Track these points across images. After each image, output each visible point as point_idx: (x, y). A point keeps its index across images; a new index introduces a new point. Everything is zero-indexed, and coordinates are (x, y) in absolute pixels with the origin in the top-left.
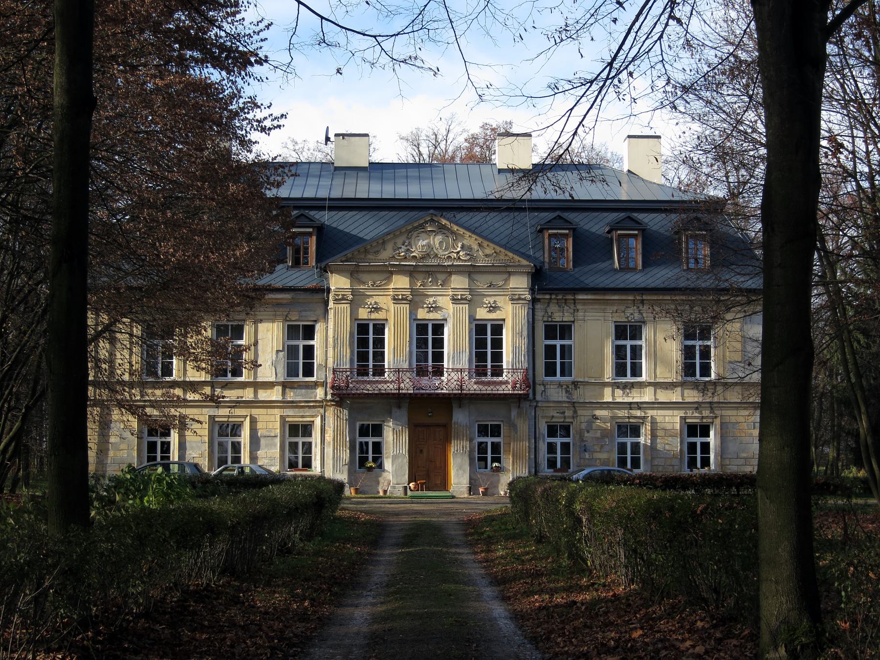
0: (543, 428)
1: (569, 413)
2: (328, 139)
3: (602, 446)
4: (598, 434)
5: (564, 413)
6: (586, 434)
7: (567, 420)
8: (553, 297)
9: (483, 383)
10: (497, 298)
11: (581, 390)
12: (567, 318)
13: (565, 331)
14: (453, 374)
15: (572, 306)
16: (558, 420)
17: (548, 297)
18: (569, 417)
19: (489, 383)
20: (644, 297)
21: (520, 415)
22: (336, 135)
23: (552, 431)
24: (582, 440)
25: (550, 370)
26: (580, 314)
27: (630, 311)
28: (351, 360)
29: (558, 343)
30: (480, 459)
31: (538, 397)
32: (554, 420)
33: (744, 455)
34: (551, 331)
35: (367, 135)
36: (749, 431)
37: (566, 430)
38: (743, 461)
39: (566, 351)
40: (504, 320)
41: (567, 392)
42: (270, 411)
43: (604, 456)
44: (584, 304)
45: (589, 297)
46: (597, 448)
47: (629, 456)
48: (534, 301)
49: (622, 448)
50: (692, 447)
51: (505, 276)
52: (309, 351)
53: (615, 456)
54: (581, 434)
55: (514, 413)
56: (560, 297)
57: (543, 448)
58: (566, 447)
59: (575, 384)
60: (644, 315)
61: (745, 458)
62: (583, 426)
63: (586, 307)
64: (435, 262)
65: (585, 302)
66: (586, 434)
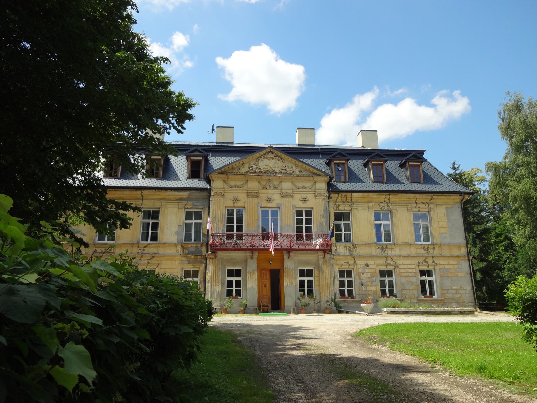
1: (351, 263)
2: (213, 130)
3: (372, 283)
4: (369, 275)
5: (348, 263)
6: (362, 275)
7: (351, 267)
13: (346, 216)
14: (285, 238)
16: (345, 267)
19: (305, 244)
22: (217, 127)
24: (360, 279)
25: (339, 239)
28: (223, 231)
29: (343, 222)
30: (301, 290)
31: (333, 252)
33: (455, 288)
34: (338, 216)
35: (233, 127)
36: (456, 274)
37: (349, 273)
38: (454, 292)
39: (348, 227)
40: (312, 208)
41: (349, 250)
42: (173, 262)
43: (373, 288)
47: (387, 288)
48: (329, 197)
49: (382, 283)
50: (423, 283)
53: (379, 288)
54: (359, 275)
57: (337, 284)
58: (350, 283)
59: (354, 246)
61: (456, 290)
62: (360, 270)
66: (362, 275)
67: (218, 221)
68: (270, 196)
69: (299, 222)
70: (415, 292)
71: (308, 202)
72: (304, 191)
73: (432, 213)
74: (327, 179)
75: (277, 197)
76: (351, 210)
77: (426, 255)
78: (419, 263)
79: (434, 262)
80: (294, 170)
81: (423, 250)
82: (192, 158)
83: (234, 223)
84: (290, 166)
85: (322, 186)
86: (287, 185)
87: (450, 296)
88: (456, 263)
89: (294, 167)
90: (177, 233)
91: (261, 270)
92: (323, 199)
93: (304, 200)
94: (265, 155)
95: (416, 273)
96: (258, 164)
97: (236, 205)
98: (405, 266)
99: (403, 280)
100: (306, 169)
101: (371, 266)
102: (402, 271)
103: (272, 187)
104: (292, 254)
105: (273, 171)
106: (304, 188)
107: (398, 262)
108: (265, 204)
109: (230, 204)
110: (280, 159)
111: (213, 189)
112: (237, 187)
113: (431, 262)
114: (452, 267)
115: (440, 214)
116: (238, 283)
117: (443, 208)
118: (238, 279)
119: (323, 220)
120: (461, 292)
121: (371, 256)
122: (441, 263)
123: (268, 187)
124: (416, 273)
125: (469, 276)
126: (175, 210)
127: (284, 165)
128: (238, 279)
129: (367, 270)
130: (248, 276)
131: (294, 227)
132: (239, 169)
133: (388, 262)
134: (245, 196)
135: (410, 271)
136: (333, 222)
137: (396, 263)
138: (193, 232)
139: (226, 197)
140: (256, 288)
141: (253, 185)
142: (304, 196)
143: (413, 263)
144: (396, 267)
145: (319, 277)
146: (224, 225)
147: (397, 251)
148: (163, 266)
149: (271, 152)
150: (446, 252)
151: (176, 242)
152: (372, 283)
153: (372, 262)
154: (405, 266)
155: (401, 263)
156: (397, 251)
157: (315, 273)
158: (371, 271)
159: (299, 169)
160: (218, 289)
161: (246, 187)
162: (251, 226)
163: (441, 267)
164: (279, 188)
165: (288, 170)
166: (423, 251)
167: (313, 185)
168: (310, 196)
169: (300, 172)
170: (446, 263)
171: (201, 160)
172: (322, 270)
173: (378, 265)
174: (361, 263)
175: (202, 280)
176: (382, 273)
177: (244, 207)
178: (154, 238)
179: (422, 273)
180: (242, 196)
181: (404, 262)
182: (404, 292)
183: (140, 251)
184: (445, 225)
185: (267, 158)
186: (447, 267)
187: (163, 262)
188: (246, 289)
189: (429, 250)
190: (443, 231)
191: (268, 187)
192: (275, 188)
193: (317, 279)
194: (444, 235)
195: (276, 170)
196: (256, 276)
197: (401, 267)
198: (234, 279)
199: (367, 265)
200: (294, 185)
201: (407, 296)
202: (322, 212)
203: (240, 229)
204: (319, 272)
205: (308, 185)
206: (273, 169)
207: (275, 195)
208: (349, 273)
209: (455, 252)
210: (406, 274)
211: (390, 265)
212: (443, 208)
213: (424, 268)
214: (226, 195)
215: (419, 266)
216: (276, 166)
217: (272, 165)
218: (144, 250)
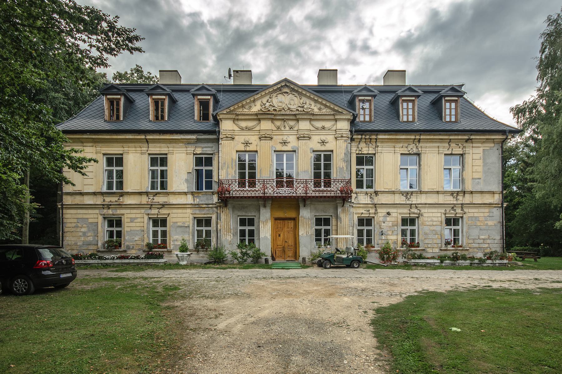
4: (390, 224)
7: (371, 215)
8: (363, 137)
9: (319, 191)
10: (327, 137)
12: (371, 151)
15: (374, 144)
17: (360, 137)
18: (372, 214)
19: (323, 191)
20: (422, 137)
23: (361, 222)
24: (381, 228)
25: (360, 184)
26: (379, 149)
27: (411, 147)
30: (317, 240)
32: (363, 215)
33: (483, 237)
36: (486, 222)
37: (369, 222)
38: (481, 241)
40: (332, 151)
41: (371, 198)
42: (184, 211)
43: (394, 238)
44: (382, 142)
45: (386, 137)
46: (390, 233)
51: (333, 123)
55: (339, 210)
56: (368, 137)
58: (369, 233)
59: (376, 193)
60: (420, 149)
63: (383, 144)
64: (288, 112)
65: (383, 141)
66: (383, 224)
68: (285, 138)
69: (317, 167)
71: (327, 145)
72: (323, 132)
73: (466, 156)
76: (375, 154)
77: (455, 202)
78: (446, 211)
79: (462, 210)
80: (312, 107)
81: (452, 197)
82: (199, 97)
84: (308, 103)
86: (304, 125)
87: (477, 246)
88: (487, 210)
90: (187, 181)
92: (345, 141)
96: (272, 101)
98: (431, 215)
101: (394, 215)
102: (426, 219)
103: (287, 128)
105: (289, 109)
107: (423, 211)
108: (279, 147)
110: (296, 95)
111: (221, 131)
112: (248, 129)
113: (459, 211)
114: (482, 215)
115: (475, 156)
116: (251, 233)
117: (480, 150)
118: (251, 228)
120: (488, 241)
121: (394, 205)
122: (470, 210)
123: (283, 129)
125: (499, 225)
127: (301, 101)
128: (251, 228)
129: (388, 219)
130: (261, 225)
131: (311, 173)
132: (250, 107)
133: (412, 210)
134: (256, 138)
135: (435, 219)
136: (354, 167)
137: (420, 211)
139: (236, 139)
140: (269, 237)
141: (266, 125)
142: (323, 138)
144: (420, 215)
145: (337, 225)
146: (235, 171)
150: (478, 199)
152: (393, 232)
153: (395, 210)
154: (431, 215)
155: (426, 211)
157: (333, 221)
158: (393, 219)
159: (319, 106)
163: (471, 215)
164: (296, 129)
165: (305, 107)
166: (451, 198)
168: (330, 138)
169: (320, 109)
170: (476, 210)
171: (209, 99)
173: (400, 214)
174: (382, 211)
175: (215, 229)
176: (404, 221)
177: (257, 151)
178: (163, 185)
180: (253, 139)
181: (430, 210)
183: (150, 200)
184: (480, 169)
185: (282, 93)
186: (476, 215)
188: (259, 239)
189: (458, 198)
190: (476, 176)
191: (283, 129)
192: (291, 128)
193: (334, 228)
194: (477, 180)
195: (292, 107)
196: (269, 225)
197: (425, 215)
198: (247, 228)
199: (389, 214)
200: (312, 126)
201: (429, 246)
204: (337, 221)
205: (328, 124)
206: (289, 106)
207: (291, 137)
208: (369, 222)
209: (488, 199)
210: (431, 223)
211: (414, 213)
212: (480, 150)
213: (451, 215)
214: (236, 137)
215: (445, 214)
216: (292, 103)
217: (287, 102)
218: (153, 199)
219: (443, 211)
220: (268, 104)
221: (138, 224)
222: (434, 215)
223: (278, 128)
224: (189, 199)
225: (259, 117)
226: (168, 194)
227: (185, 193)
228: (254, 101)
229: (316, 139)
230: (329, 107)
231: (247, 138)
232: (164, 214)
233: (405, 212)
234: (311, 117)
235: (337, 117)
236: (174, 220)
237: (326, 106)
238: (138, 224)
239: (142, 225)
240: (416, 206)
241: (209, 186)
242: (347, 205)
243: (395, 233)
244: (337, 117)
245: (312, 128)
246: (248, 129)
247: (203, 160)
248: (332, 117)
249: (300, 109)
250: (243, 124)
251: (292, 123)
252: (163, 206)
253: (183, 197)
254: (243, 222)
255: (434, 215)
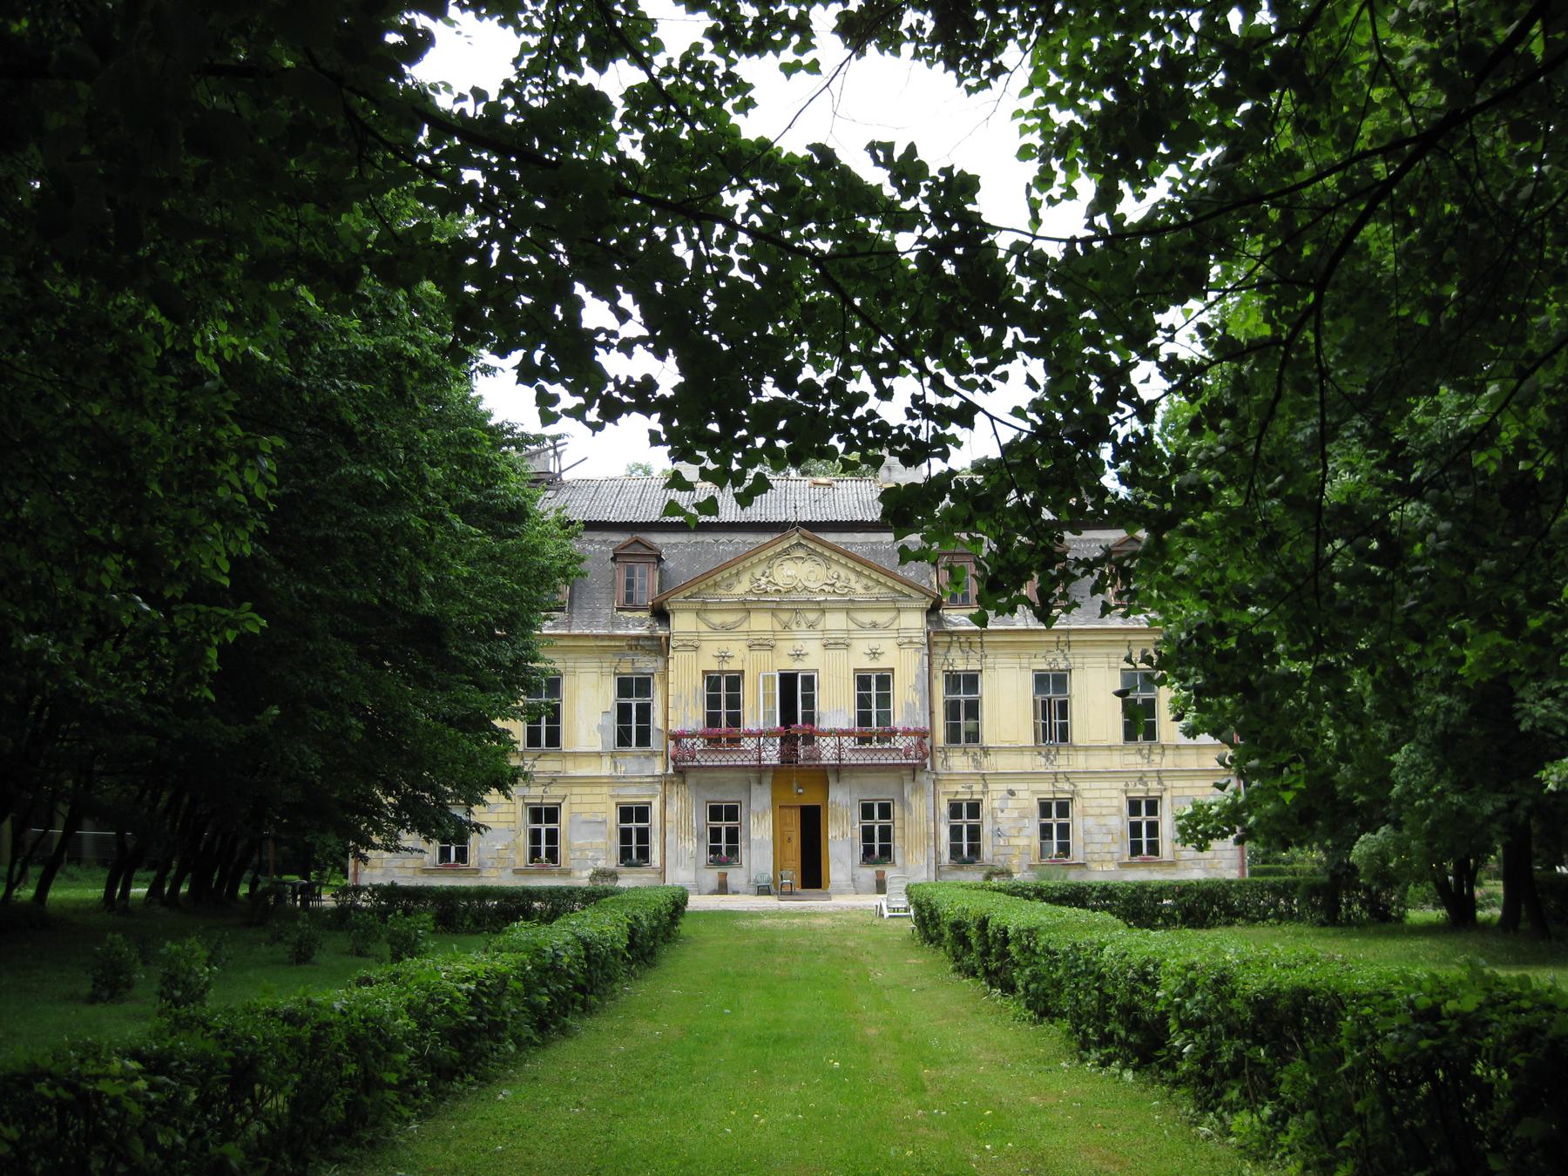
0: (944, 809)
4: (1016, 814)
11: (992, 759)
12: (974, 666)
13: (972, 681)
19: (876, 750)
21: (915, 791)
23: (955, 810)
25: (953, 736)
31: (939, 768)
34: (953, 681)
42: (597, 790)
43: (1022, 842)
51: (894, 614)
52: (644, 711)
55: (908, 788)
57: (945, 832)
62: (996, 804)
64: (804, 596)
67: (687, 704)
68: (798, 645)
70: (1114, 848)
71: (882, 658)
74: (927, 603)
75: (813, 648)
79: (1160, 781)
80: (853, 584)
83: (723, 691)
85: (914, 621)
86: (836, 622)
89: (853, 577)
90: (601, 728)
91: (779, 808)
92: (917, 650)
93: (874, 654)
94: (786, 551)
95: (1119, 809)
97: (725, 667)
98: (1097, 794)
99: (1090, 822)
100: (878, 582)
101: (1020, 795)
103: (804, 626)
104: (843, 774)
106: (875, 625)
107: (1081, 785)
109: (713, 666)
112: (726, 628)
113: (1153, 785)
119: (915, 698)
122: (1176, 784)
123: (794, 627)
124: (1119, 809)
126: (593, 678)
129: (1011, 803)
130: (753, 820)
132: (730, 586)
134: (743, 645)
135: (1104, 802)
138: (632, 725)
141: (761, 623)
142: (874, 644)
143: (1115, 785)
147: (1079, 762)
148: (575, 799)
149: (799, 544)
151: (599, 749)
153: (1024, 786)
154: (1097, 794)
155: (1086, 785)
156: (1079, 762)
159: (865, 581)
160: (691, 845)
161: (745, 627)
162: (760, 708)
163: (1176, 792)
164: (819, 627)
167: (894, 619)
169: (867, 588)
170: (1188, 783)
172: (910, 805)
173: (1034, 792)
174: (998, 788)
179: (1134, 807)
181: (1095, 785)
182: (1088, 850)
187: (576, 790)
191: (794, 627)
192: (811, 626)
195: (811, 585)
197: (1086, 794)
199: (1011, 793)
200: (852, 620)
202: (912, 680)
203: (735, 720)
205: (882, 618)
210: (1097, 811)
211: (1063, 791)
217: (802, 576)
219: (1122, 785)
220: (764, 580)
221: (503, 817)
222: (1104, 794)
223: (786, 627)
224: (605, 768)
225: (746, 607)
226: (565, 755)
227: (599, 755)
228: (737, 574)
229: (861, 647)
230: (885, 585)
231: (724, 646)
232: (556, 797)
233: (1045, 789)
234: (850, 606)
235: (899, 605)
236: (576, 808)
237: (878, 582)
238: (503, 817)
239: (511, 818)
240: (1067, 776)
241: (644, 739)
242: (921, 777)
243: (1026, 832)
244: (899, 605)
245: (853, 626)
246: (726, 628)
247: (633, 687)
248: (890, 605)
249: (827, 588)
250: (717, 619)
251: (812, 616)
252: (553, 780)
253: (594, 760)
254: (715, 813)
255: (1104, 794)
